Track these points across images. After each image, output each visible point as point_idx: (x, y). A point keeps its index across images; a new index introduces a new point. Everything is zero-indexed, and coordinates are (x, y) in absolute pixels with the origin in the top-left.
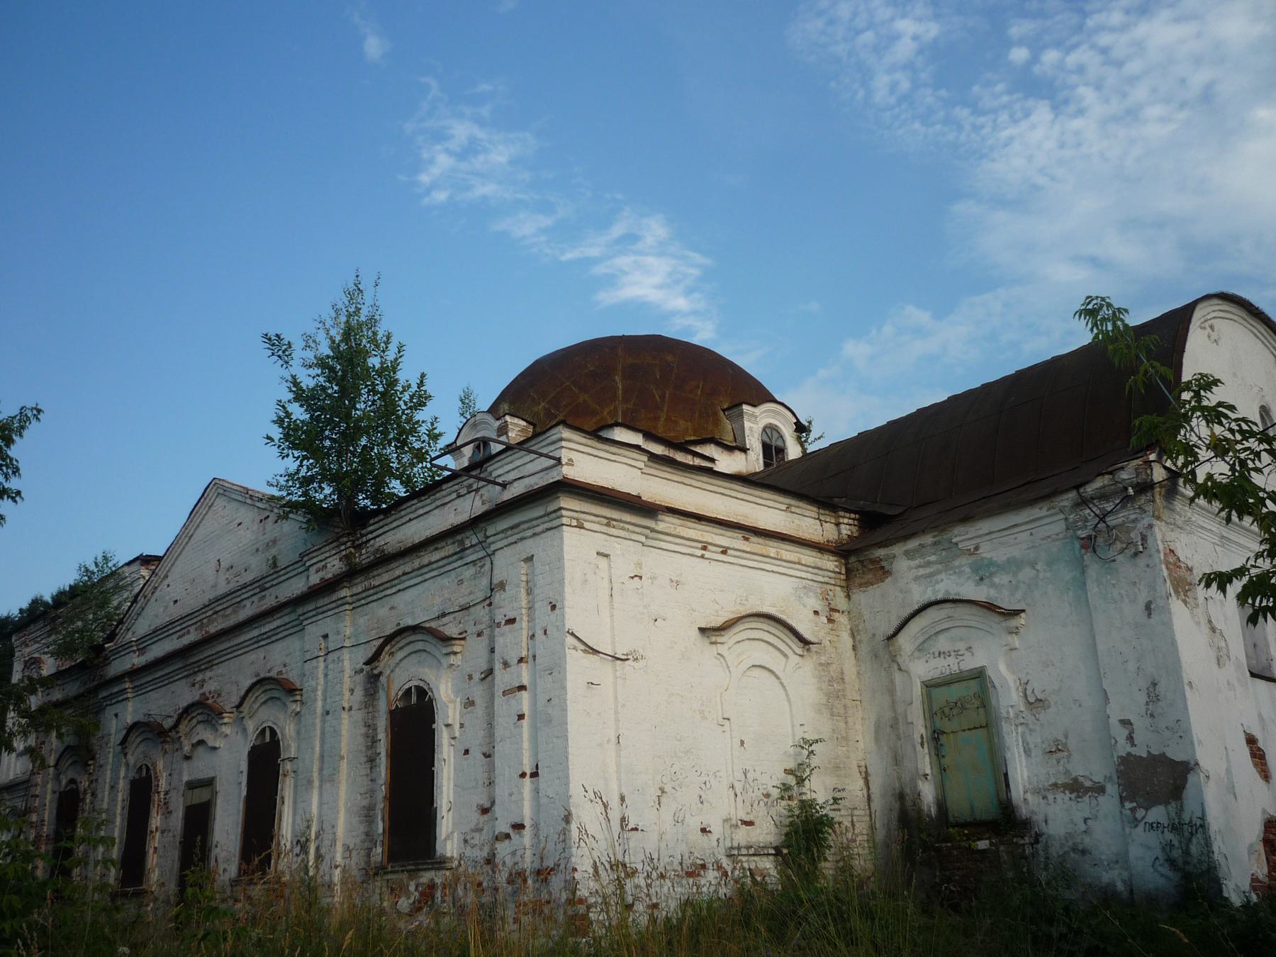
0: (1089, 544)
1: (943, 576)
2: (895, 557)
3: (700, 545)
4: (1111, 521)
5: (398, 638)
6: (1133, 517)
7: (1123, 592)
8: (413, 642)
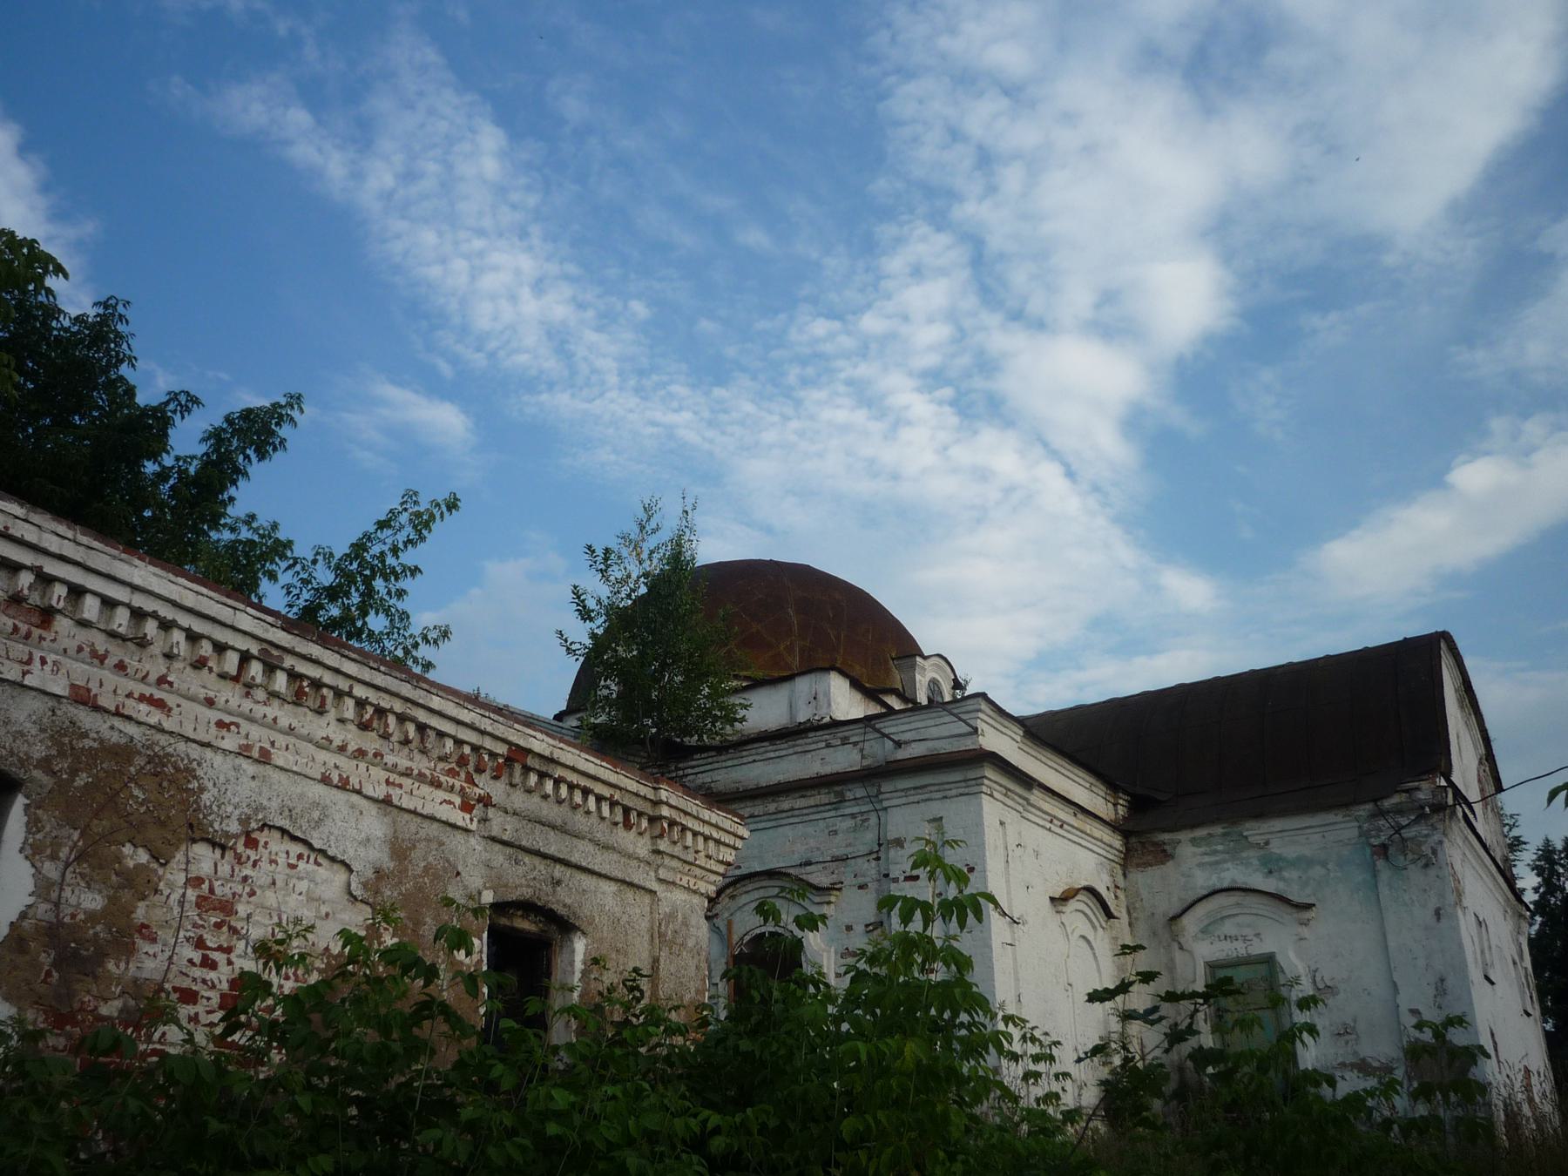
0: (1383, 850)
1: (1229, 865)
2: (1180, 842)
3: (1049, 818)
4: (1406, 833)
5: (747, 881)
6: (1426, 832)
7: (1414, 898)
8: (765, 887)
